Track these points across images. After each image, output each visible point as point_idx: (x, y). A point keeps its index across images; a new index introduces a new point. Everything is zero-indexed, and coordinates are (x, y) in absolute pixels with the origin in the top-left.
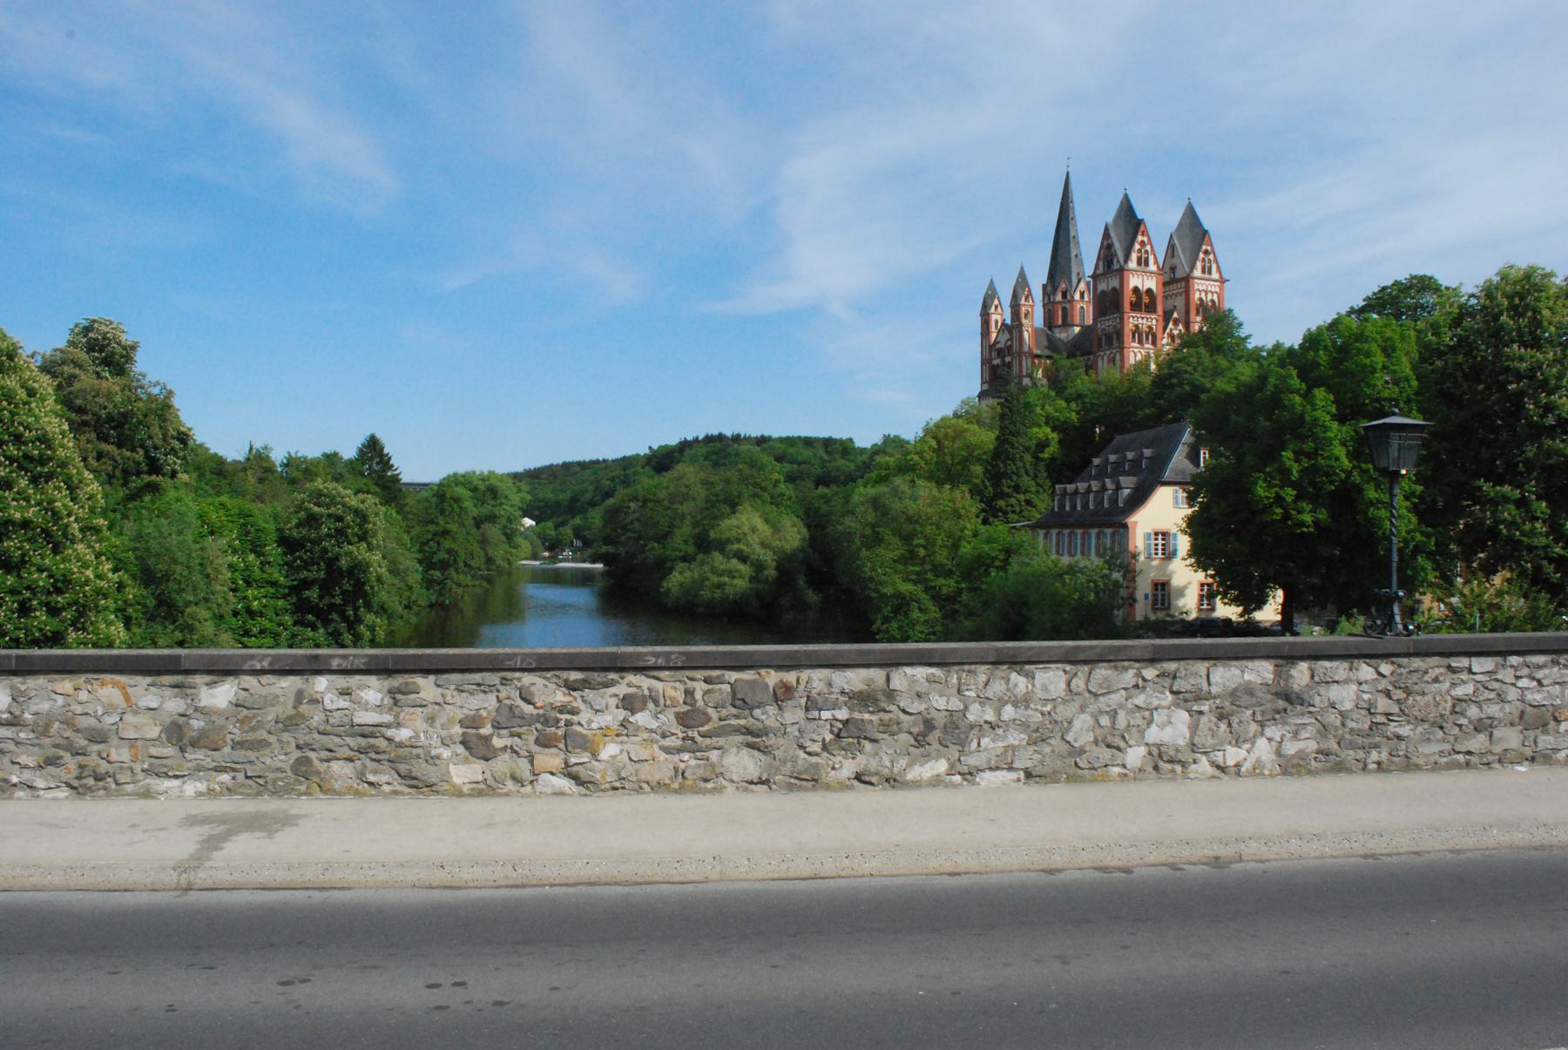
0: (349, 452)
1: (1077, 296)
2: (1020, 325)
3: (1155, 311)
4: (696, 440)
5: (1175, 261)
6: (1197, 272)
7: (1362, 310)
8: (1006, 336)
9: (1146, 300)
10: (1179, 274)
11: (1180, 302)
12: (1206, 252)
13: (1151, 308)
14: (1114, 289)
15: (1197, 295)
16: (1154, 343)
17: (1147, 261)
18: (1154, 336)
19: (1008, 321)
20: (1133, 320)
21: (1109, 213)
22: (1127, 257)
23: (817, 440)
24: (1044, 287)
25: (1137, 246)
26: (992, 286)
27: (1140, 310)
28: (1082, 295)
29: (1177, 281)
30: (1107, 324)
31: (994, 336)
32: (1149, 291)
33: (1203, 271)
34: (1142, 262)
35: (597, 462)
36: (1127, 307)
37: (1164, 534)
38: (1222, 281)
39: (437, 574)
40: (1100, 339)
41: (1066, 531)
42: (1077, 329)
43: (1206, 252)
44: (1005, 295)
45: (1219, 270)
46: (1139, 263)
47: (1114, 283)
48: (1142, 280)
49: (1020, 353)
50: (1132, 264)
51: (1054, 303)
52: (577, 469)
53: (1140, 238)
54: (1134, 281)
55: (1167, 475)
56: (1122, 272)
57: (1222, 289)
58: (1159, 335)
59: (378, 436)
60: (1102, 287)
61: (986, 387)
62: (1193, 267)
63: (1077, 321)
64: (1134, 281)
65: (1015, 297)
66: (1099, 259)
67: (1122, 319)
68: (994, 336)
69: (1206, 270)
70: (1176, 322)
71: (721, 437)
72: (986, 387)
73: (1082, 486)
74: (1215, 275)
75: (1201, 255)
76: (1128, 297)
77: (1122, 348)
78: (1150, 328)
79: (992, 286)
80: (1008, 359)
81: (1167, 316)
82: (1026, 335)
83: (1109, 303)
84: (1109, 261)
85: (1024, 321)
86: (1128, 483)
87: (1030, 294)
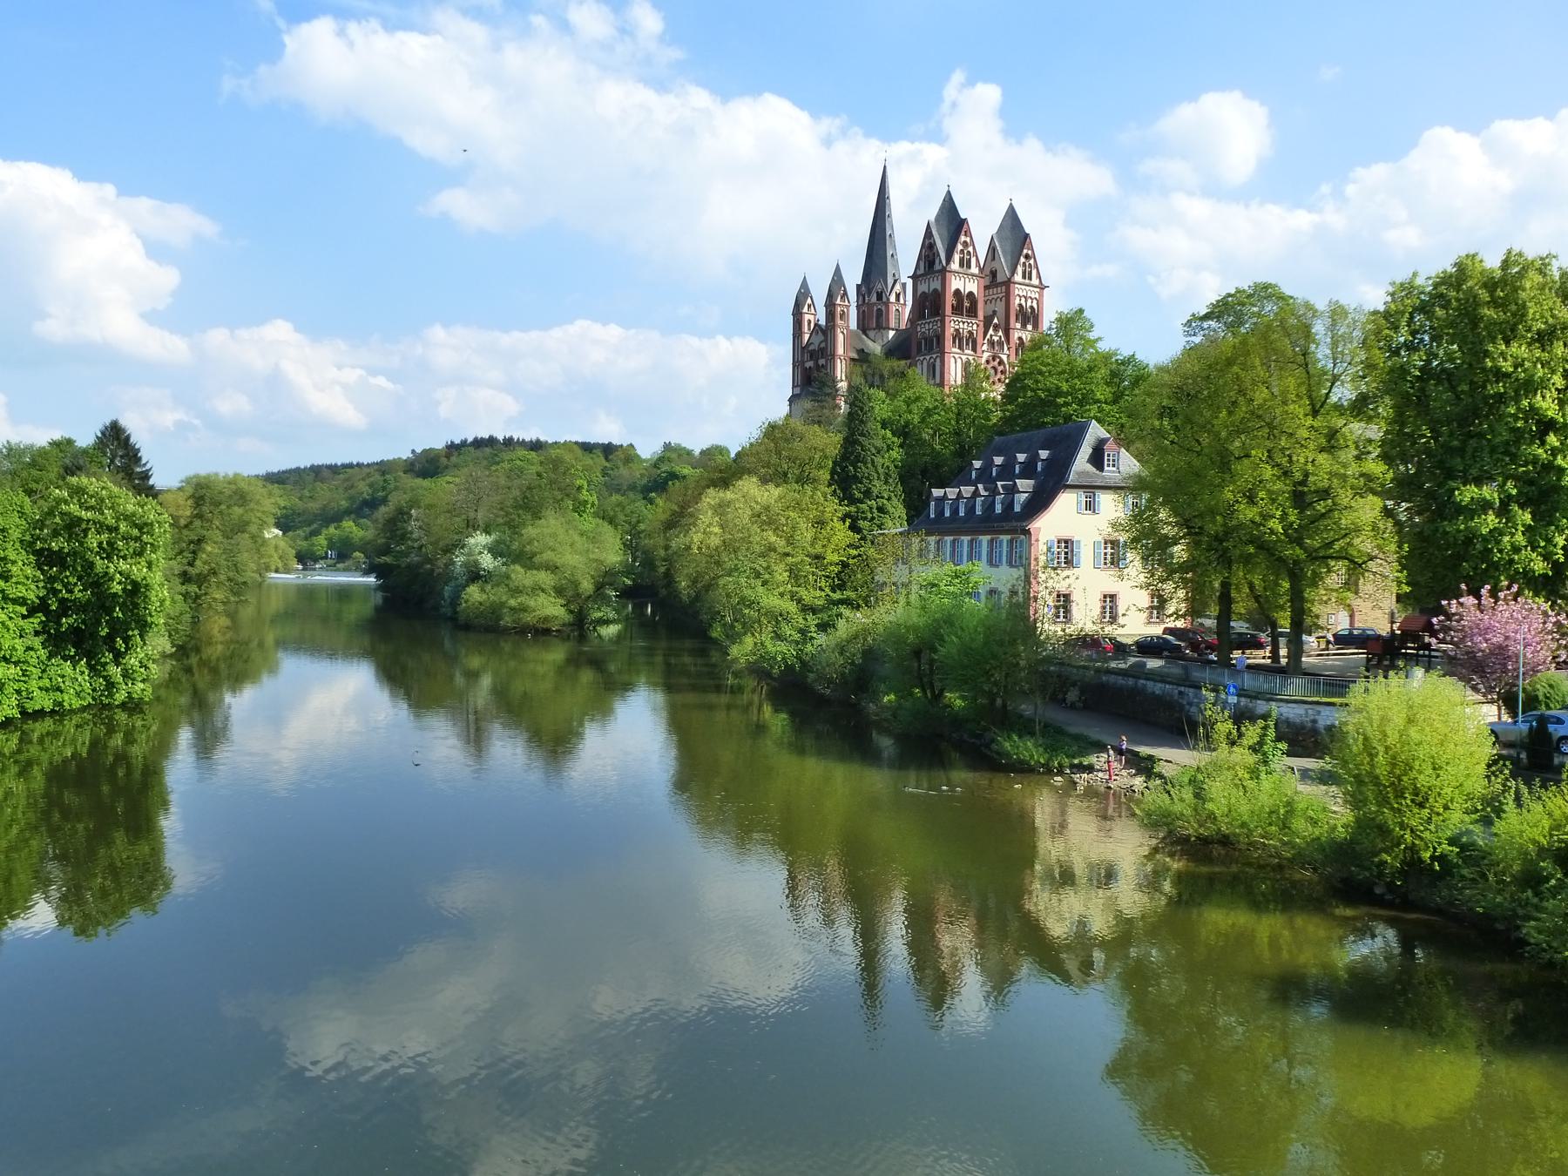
0: (85, 438)
1: (893, 298)
4: (464, 443)
5: (995, 265)
6: (1018, 277)
7: (1207, 317)
9: (967, 304)
12: (1027, 257)
13: (972, 312)
14: (935, 290)
16: (974, 350)
17: (969, 261)
19: (823, 322)
20: (954, 324)
21: (932, 212)
22: (949, 258)
23: (596, 446)
24: (858, 286)
25: (960, 247)
26: (804, 284)
28: (898, 296)
29: (996, 282)
30: (925, 328)
31: (806, 337)
32: (971, 293)
35: (350, 466)
36: (948, 310)
37: (1066, 542)
38: (1042, 287)
39: (193, 588)
41: (949, 539)
42: (891, 333)
43: (1027, 257)
44: (819, 295)
46: (961, 265)
47: (936, 285)
48: (963, 283)
50: (955, 266)
51: (870, 305)
52: (326, 473)
53: (963, 238)
54: (956, 284)
55: (1072, 478)
56: (944, 271)
57: (1041, 295)
58: (980, 340)
59: (123, 423)
60: (923, 288)
61: (798, 391)
62: (1013, 272)
63: (892, 325)
64: (956, 284)
67: (943, 322)
68: (806, 337)
70: (996, 328)
71: (492, 441)
72: (798, 391)
73: (952, 493)
74: (1035, 281)
75: (1022, 260)
76: (950, 300)
77: (942, 353)
78: (971, 333)
79: (804, 284)
80: (822, 362)
81: (988, 322)
82: (840, 338)
83: (929, 305)
84: (929, 263)
85: (839, 322)
86: (1025, 485)
87: (845, 293)
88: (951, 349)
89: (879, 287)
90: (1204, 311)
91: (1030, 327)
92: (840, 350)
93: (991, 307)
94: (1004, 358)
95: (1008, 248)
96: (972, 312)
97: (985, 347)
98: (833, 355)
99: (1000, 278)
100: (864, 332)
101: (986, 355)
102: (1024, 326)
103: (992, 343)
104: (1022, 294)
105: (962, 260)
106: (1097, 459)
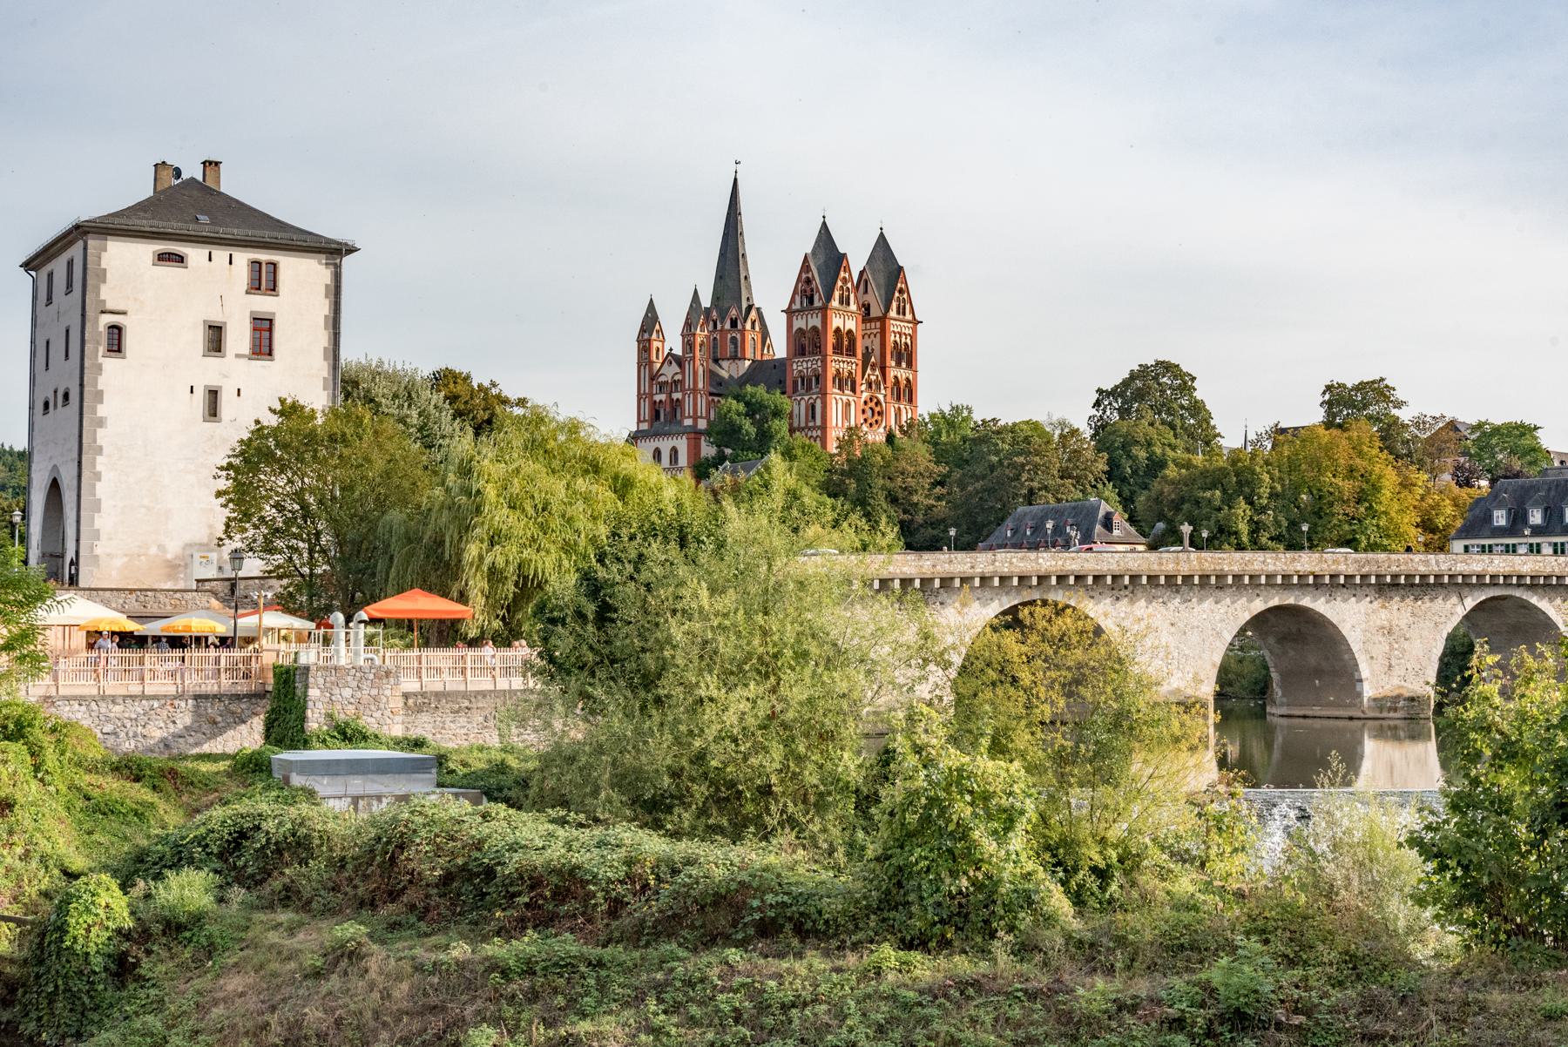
1: (748, 326)
3: (854, 355)
6: (893, 313)
8: (675, 368)
11: (877, 347)
12: (901, 291)
13: (851, 352)
14: (814, 328)
16: (853, 390)
20: (837, 364)
21: (807, 243)
22: (829, 297)
25: (840, 283)
28: (753, 323)
30: (802, 366)
32: (850, 331)
34: (845, 301)
36: (830, 350)
38: (915, 322)
40: (795, 383)
42: (747, 363)
43: (901, 291)
46: (841, 302)
47: (815, 321)
48: (844, 320)
49: (695, 390)
50: (835, 303)
53: (842, 274)
54: (836, 322)
56: (824, 309)
57: (915, 331)
60: (799, 323)
61: (645, 426)
62: (888, 308)
63: (749, 354)
64: (836, 322)
65: (689, 325)
67: (824, 362)
69: (901, 311)
70: (873, 366)
74: (909, 317)
77: (824, 394)
80: (676, 396)
83: (806, 343)
88: (833, 390)
89: (734, 313)
92: (700, 385)
93: (868, 342)
94: (881, 397)
95: (882, 281)
96: (851, 352)
100: (716, 361)
101: (865, 395)
102: (899, 364)
103: (870, 385)
104: (896, 327)
105: (841, 297)
106: (1108, 523)
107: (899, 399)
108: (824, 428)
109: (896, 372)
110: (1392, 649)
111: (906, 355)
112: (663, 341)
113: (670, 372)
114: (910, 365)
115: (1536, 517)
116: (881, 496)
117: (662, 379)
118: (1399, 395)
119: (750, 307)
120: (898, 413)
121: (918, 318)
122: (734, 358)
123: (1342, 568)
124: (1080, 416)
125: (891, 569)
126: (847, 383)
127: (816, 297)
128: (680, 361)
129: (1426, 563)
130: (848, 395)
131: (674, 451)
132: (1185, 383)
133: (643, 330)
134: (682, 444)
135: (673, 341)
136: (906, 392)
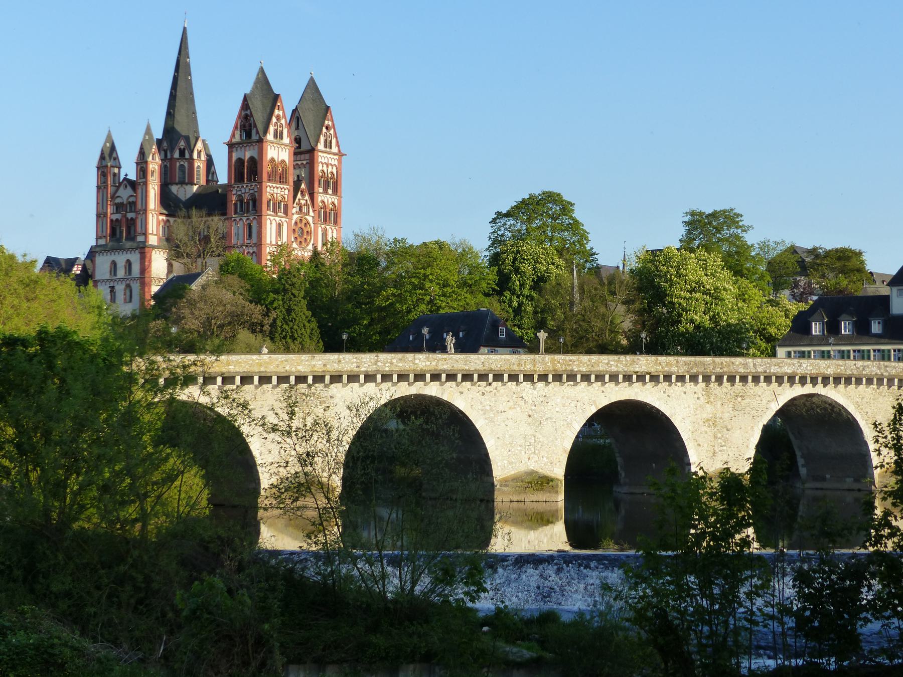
1: (195, 156)
2: (146, 184)
3: (286, 183)
6: (321, 146)
7: (508, 215)
8: (129, 191)
10: (304, 147)
15: (320, 168)
16: (286, 213)
17: (282, 132)
18: (286, 207)
25: (274, 120)
26: (109, 138)
27: (276, 182)
28: (199, 153)
32: (283, 161)
33: (326, 146)
34: (278, 135)
36: (265, 176)
38: (340, 154)
42: (195, 188)
43: (327, 128)
45: (338, 145)
46: (275, 136)
50: (270, 136)
53: (276, 112)
56: (261, 141)
61: (102, 242)
62: (318, 141)
65: (142, 154)
66: (236, 128)
69: (328, 144)
74: (335, 149)
75: (324, 130)
76: (266, 169)
77: (259, 216)
79: (109, 138)
80: (130, 215)
81: (296, 189)
90: (504, 212)
91: (330, 191)
94: (310, 219)
97: (294, 210)
98: (145, 211)
99: (304, 147)
101: (295, 217)
102: (325, 191)
107: (325, 220)
108: (259, 245)
109: (324, 198)
110: (715, 437)
111: (333, 184)
112: (119, 168)
113: (125, 194)
114: (335, 192)
115: (845, 328)
116: (304, 303)
117: (118, 201)
118: (745, 221)
119: (197, 139)
120: (325, 234)
121: (343, 151)
122: (182, 183)
123: (675, 369)
124: (478, 239)
125: (287, 368)
126: (280, 207)
127: (254, 132)
128: (133, 184)
129: (745, 365)
130: (280, 218)
131: (129, 263)
132: (566, 208)
133: (102, 157)
134: (135, 257)
135: (129, 170)
136: (331, 216)
